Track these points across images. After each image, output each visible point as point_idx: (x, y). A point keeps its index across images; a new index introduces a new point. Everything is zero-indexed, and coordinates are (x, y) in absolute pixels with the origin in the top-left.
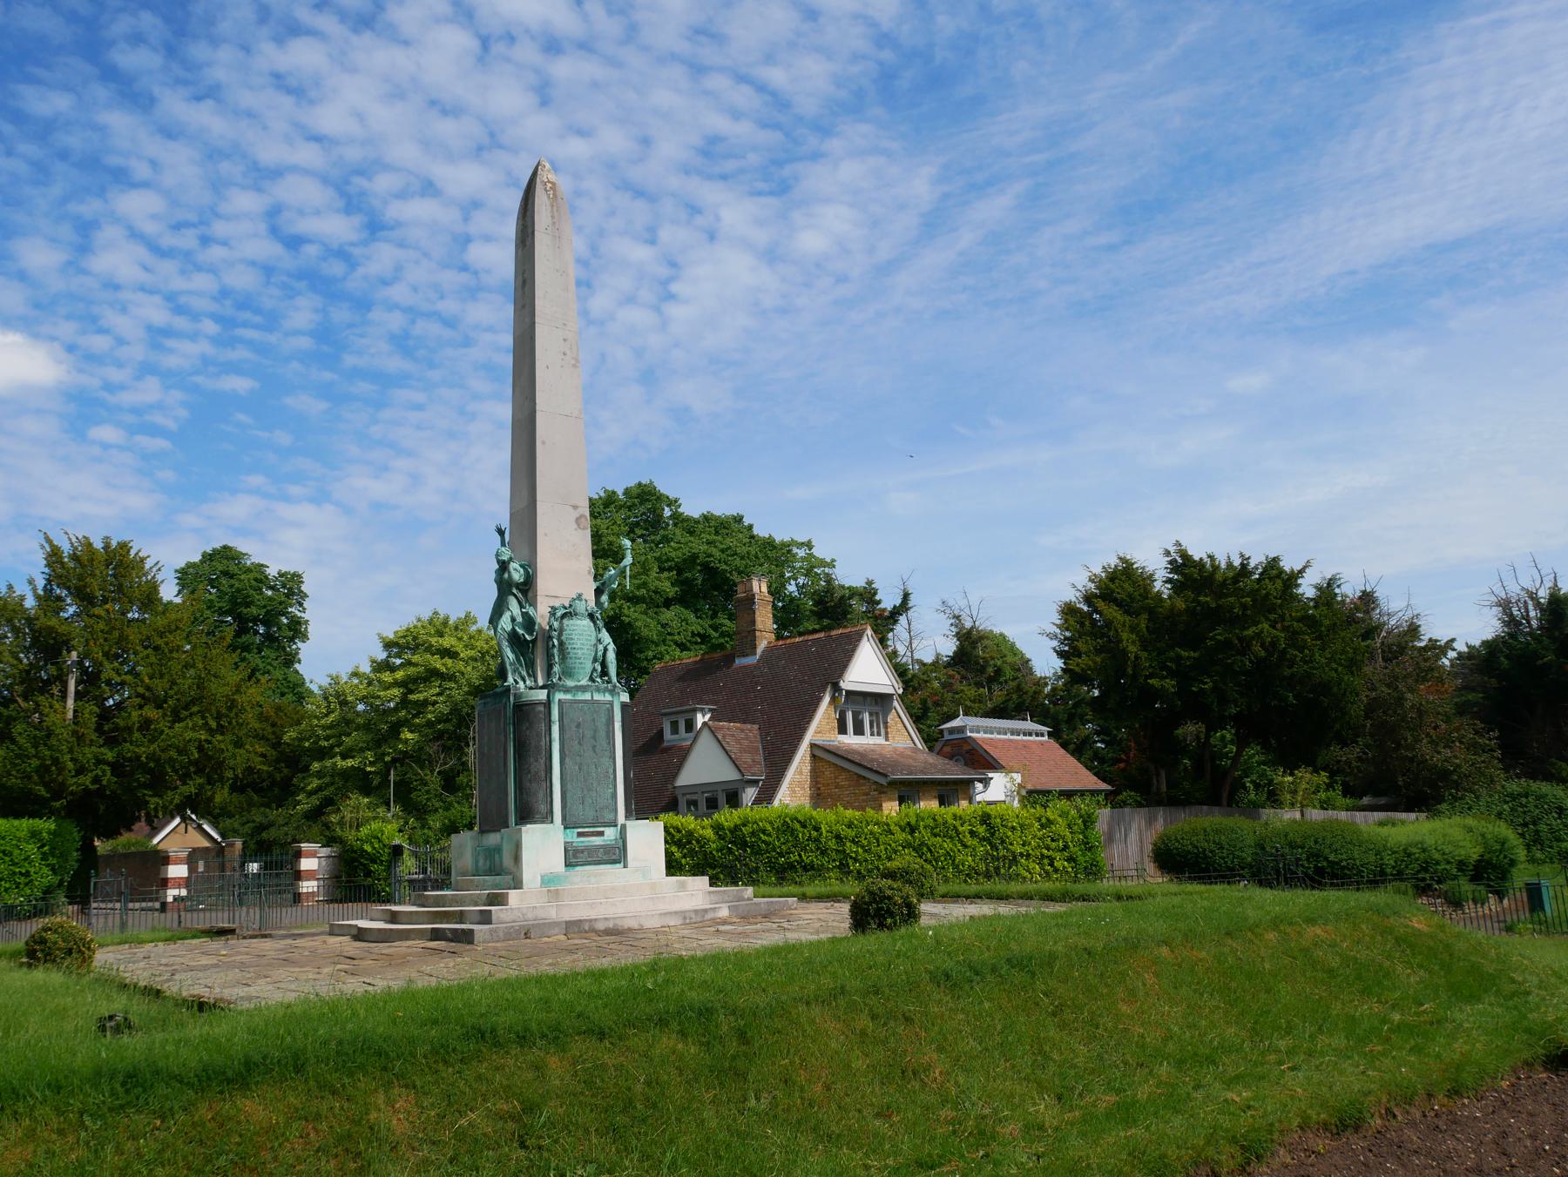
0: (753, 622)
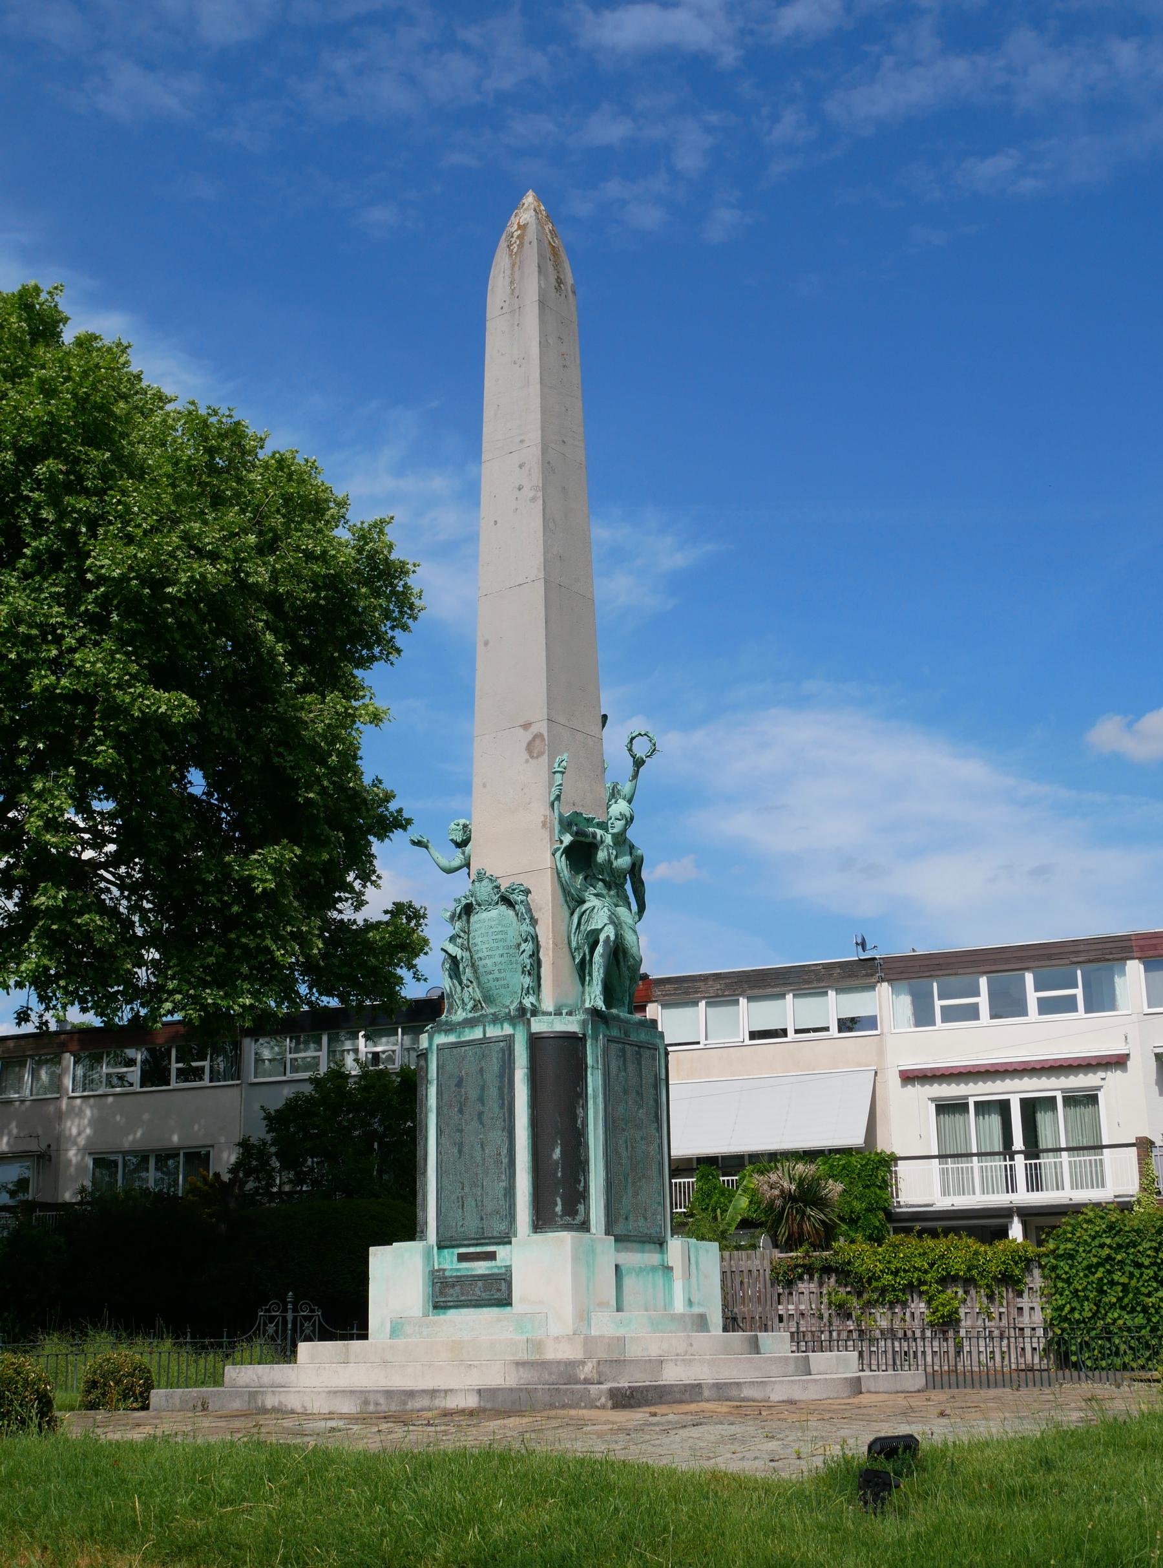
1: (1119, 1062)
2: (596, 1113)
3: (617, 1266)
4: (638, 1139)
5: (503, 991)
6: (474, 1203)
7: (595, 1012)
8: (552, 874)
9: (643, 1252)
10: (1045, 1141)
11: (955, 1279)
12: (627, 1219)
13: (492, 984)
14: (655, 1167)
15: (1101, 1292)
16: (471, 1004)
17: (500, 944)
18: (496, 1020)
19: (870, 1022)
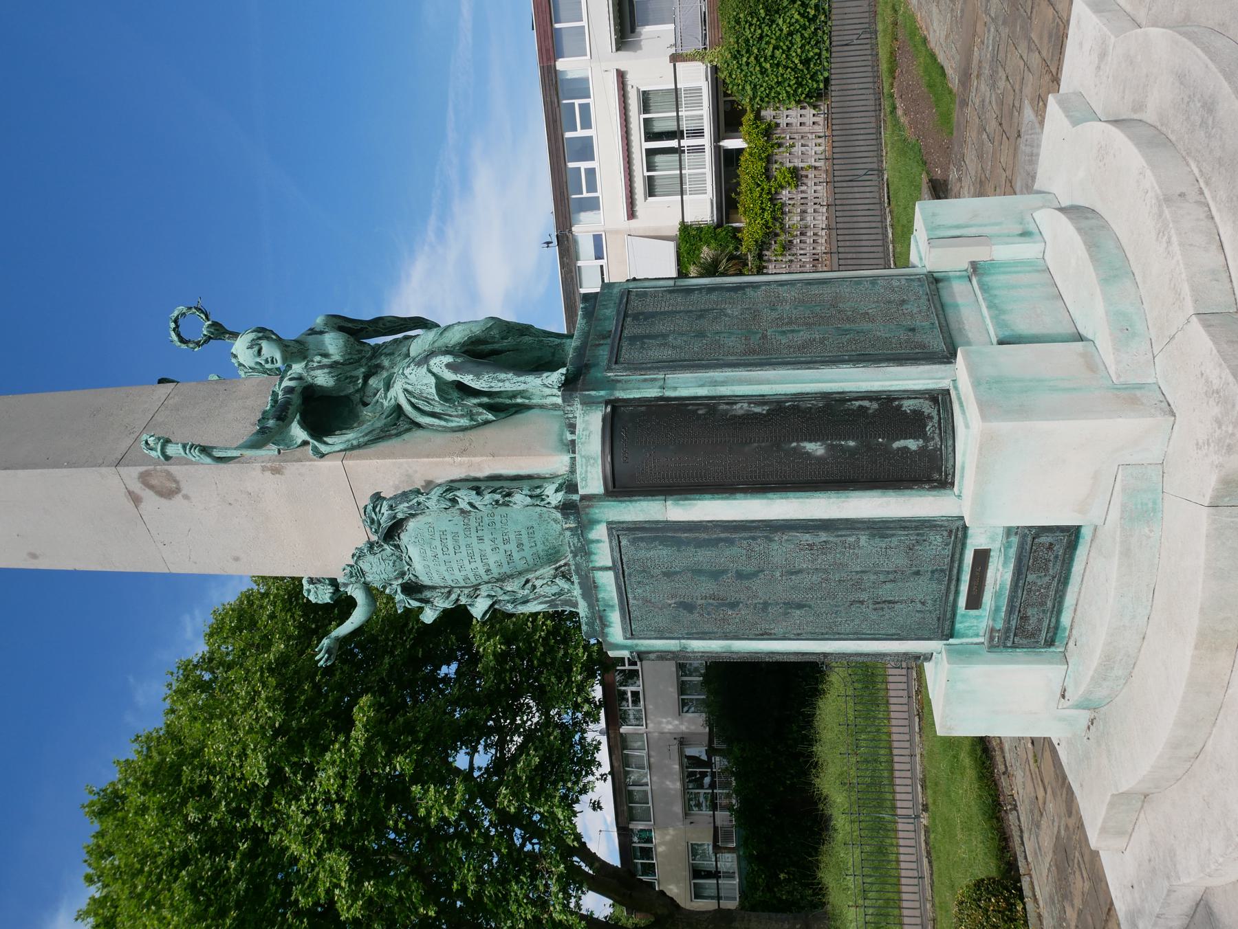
1: (621, 75)
2: (741, 382)
3: (1001, 343)
4: (775, 315)
5: (538, 537)
6: (889, 586)
7: (569, 385)
8: (351, 458)
9: (956, 306)
10: (672, 126)
11: (767, 170)
12: (913, 330)
13: (528, 552)
14: (815, 290)
15: (778, 65)
16: (561, 583)
17: (462, 541)
18: (584, 550)
19: (597, 239)
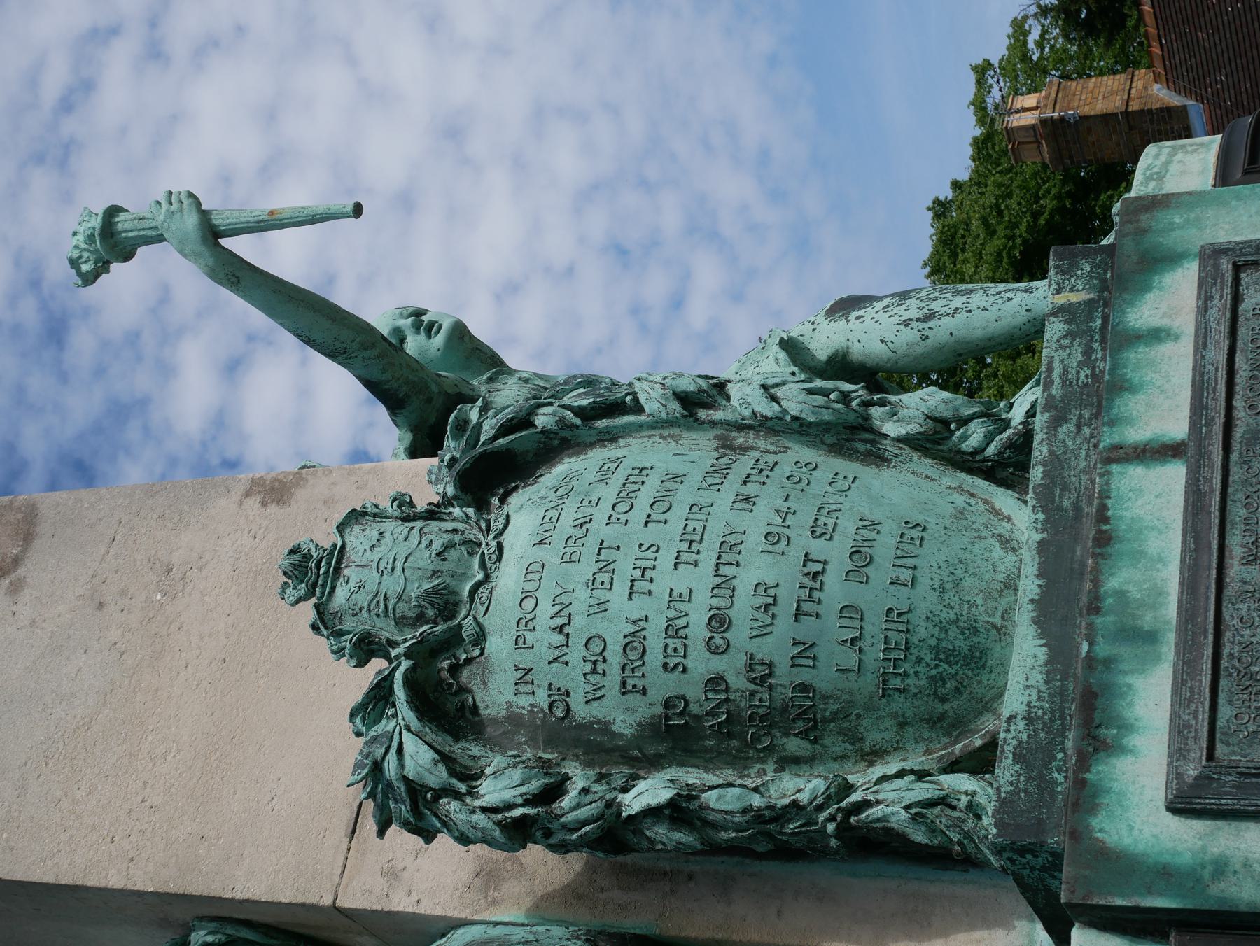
0: (1106, 118)
5: (932, 558)
17: (685, 495)
